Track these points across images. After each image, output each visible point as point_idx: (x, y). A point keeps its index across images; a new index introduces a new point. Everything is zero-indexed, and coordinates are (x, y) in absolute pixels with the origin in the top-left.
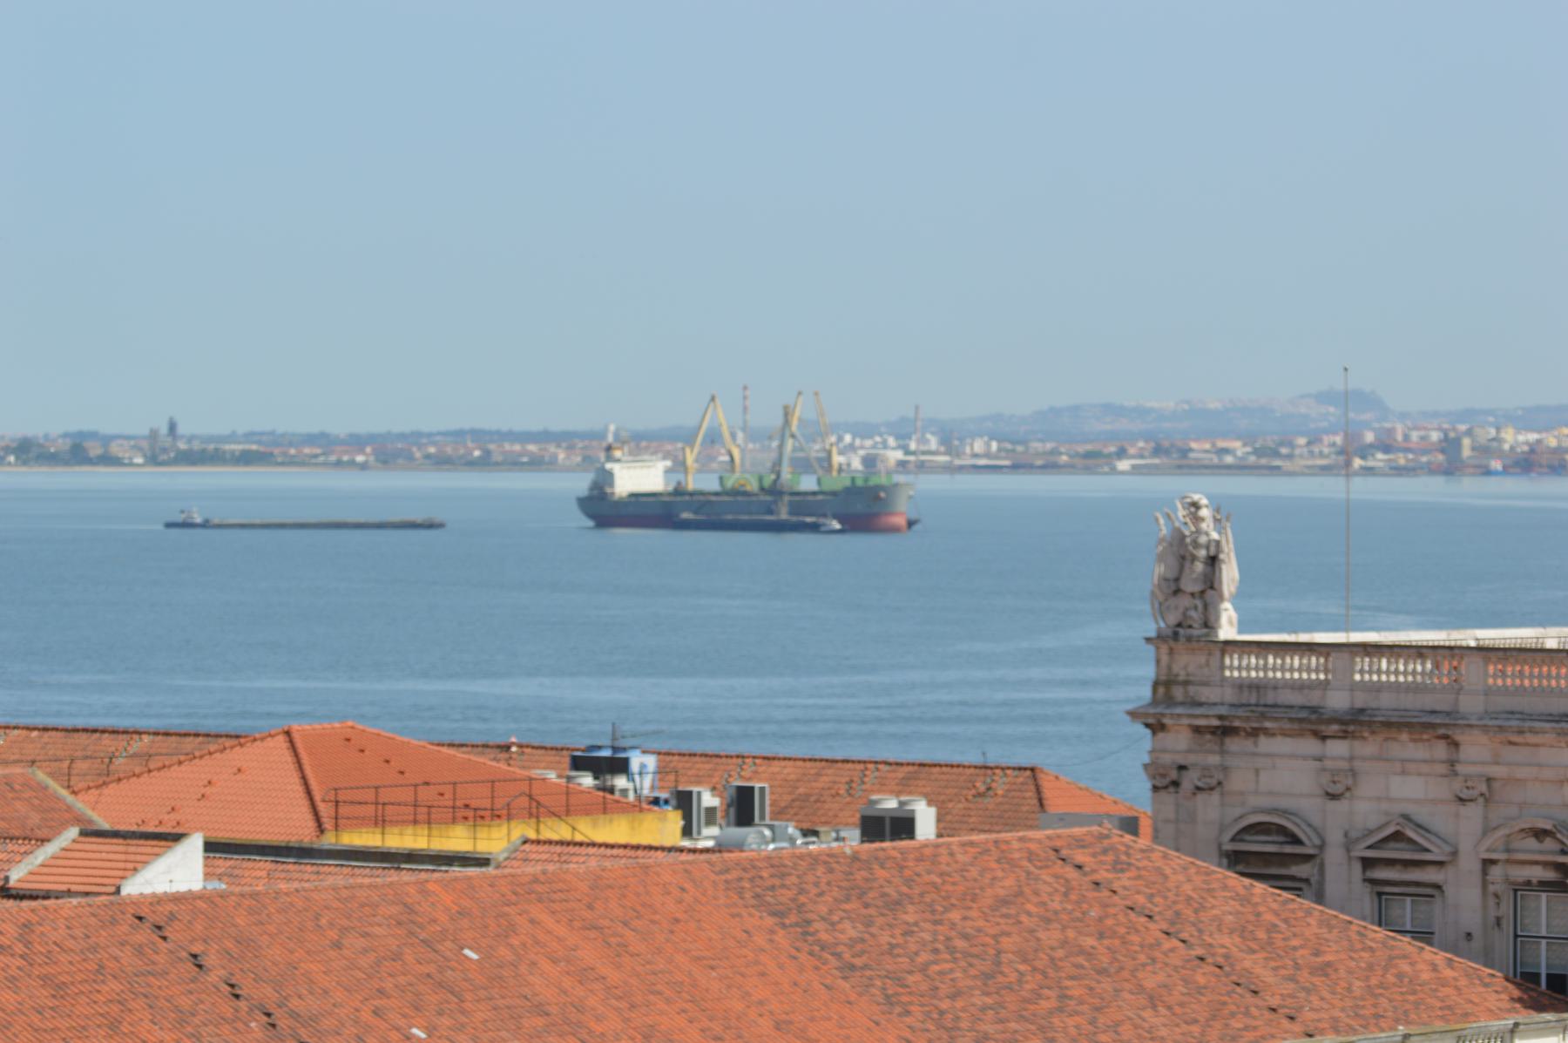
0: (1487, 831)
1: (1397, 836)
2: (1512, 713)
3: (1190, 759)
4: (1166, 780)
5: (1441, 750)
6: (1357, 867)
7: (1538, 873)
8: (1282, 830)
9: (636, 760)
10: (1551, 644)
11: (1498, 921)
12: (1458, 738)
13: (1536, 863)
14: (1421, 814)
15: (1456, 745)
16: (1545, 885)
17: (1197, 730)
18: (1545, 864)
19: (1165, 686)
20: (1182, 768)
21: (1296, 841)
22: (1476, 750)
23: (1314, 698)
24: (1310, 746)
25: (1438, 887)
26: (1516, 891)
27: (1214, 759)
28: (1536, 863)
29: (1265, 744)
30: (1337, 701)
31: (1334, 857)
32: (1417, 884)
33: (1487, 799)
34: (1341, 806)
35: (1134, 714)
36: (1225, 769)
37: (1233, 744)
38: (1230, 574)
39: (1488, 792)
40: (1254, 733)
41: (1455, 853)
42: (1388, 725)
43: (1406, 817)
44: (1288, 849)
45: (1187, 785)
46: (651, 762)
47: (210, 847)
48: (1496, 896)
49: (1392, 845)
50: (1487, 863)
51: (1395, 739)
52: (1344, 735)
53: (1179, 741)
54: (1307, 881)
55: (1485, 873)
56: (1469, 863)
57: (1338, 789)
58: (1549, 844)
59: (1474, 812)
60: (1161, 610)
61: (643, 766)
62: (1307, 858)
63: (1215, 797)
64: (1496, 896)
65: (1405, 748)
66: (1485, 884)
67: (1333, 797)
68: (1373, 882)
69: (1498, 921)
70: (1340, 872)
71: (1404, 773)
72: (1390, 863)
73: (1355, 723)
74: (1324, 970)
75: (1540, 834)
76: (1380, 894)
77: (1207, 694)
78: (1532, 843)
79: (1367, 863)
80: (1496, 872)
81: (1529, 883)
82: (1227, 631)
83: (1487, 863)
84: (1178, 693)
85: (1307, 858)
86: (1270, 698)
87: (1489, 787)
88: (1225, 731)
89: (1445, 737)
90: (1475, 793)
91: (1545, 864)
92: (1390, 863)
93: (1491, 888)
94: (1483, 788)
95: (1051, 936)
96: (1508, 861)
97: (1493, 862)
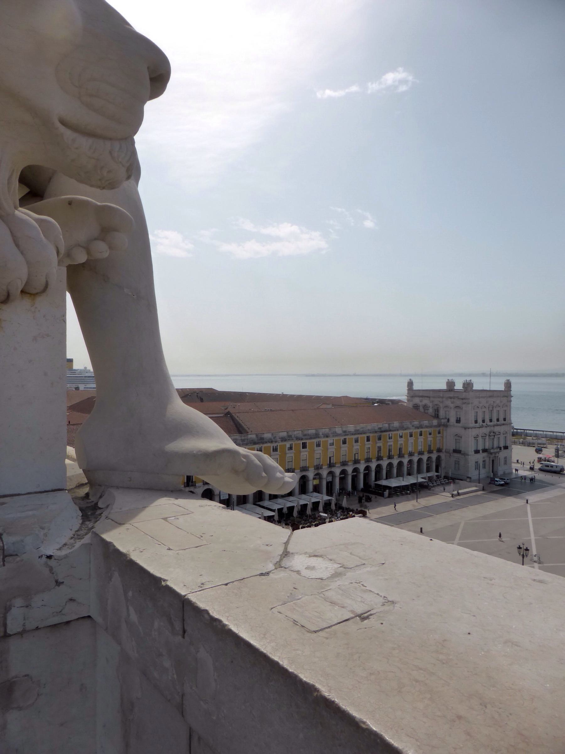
1: (425, 405)
4: (408, 400)
5: (428, 398)
7: (436, 408)
22: (432, 399)
39: (433, 402)
43: (426, 404)
47: (332, 405)
56: (431, 407)
65: (426, 398)
67: (421, 402)
73: (422, 397)
76: (424, 409)
78: (436, 406)
80: (433, 408)
85: (419, 407)
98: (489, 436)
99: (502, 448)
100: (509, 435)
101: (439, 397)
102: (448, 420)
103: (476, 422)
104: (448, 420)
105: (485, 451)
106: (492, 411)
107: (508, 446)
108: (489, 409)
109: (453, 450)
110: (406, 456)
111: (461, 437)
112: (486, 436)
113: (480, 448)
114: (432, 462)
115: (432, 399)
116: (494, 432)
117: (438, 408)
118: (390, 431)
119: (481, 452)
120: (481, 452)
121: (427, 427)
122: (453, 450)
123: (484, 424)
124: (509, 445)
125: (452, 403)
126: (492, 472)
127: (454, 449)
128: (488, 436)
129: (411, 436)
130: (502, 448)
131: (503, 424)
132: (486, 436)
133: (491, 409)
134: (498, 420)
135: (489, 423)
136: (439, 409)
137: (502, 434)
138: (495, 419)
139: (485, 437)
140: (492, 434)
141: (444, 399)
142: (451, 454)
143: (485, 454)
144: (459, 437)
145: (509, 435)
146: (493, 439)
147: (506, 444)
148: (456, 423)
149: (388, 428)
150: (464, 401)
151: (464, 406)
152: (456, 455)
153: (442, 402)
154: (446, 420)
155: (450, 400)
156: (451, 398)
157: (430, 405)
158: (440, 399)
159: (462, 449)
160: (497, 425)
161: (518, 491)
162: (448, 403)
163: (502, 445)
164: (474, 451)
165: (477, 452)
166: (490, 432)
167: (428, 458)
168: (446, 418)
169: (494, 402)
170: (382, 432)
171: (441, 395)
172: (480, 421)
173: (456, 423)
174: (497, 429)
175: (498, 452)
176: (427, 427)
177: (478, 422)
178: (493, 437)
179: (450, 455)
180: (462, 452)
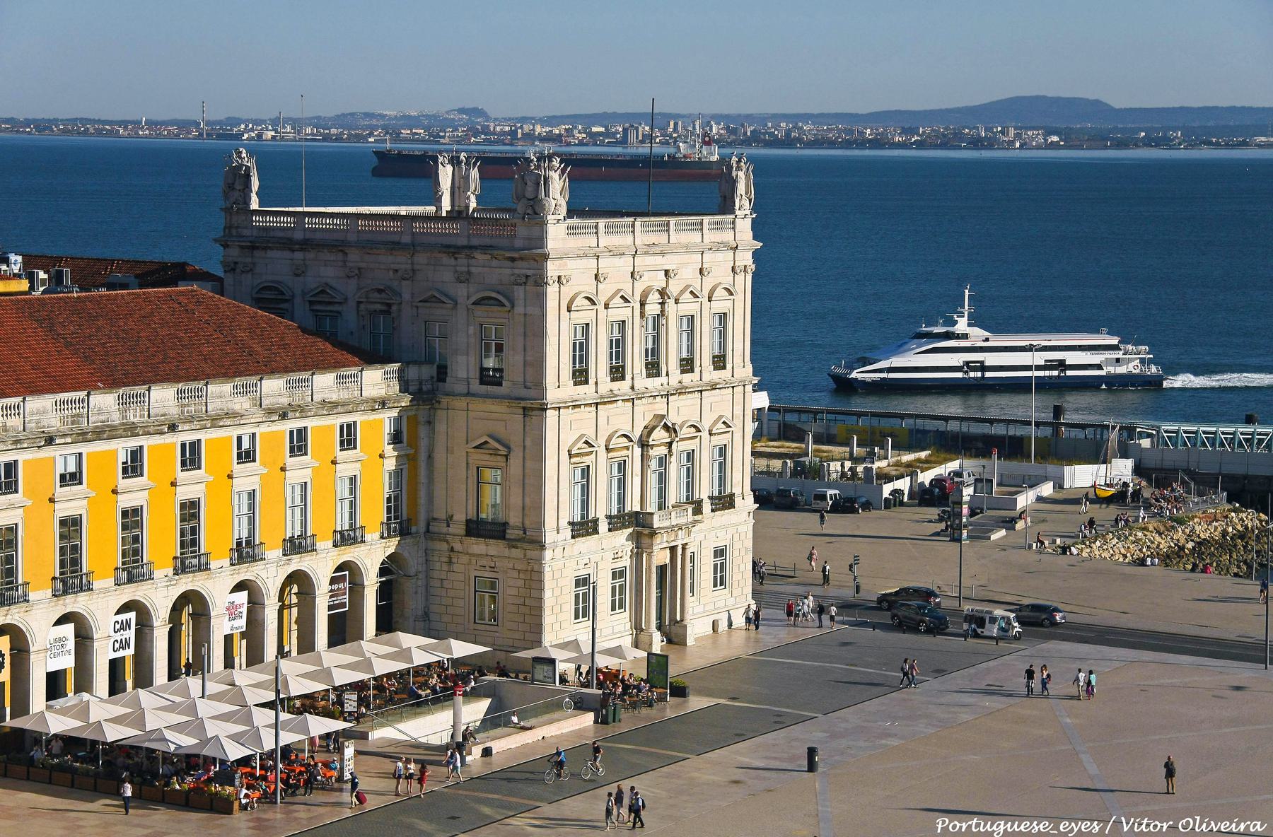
0: (359, 289)
1: (323, 292)
2: (368, 241)
3: (239, 260)
4: (231, 268)
5: (340, 256)
6: (307, 304)
7: (378, 307)
8: (277, 289)
9: (13, 257)
10: (403, 213)
11: (364, 327)
12: (347, 251)
13: (379, 303)
14: (333, 283)
15: (346, 254)
16: (382, 312)
17: (242, 247)
18: (382, 303)
19: (229, 228)
20: (236, 263)
21: (282, 293)
22: (354, 256)
23: (289, 234)
24: (287, 254)
25: (338, 312)
26: (370, 314)
27: (249, 260)
28: (379, 303)
29: (270, 254)
30: (298, 236)
31: (298, 300)
32: (331, 311)
33: (359, 276)
34: (301, 279)
35: (216, 240)
36: (254, 264)
37: (257, 253)
38: (255, 184)
39: (360, 272)
40: (265, 249)
41: (346, 299)
42: (318, 245)
43: (327, 284)
44: (280, 297)
45: (238, 270)
46: (19, 259)
48: (363, 316)
49: (321, 295)
50: (359, 303)
51: (322, 252)
52: (302, 250)
53: (234, 252)
54: (287, 310)
55: (358, 307)
56: (352, 303)
57: (300, 272)
58: (383, 295)
59: (353, 282)
60: (226, 196)
61: (16, 261)
62: (286, 301)
63: (249, 275)
64: (363, 316)
66: (358, 311)
67: (297, 275)
68: (313, 310)
69: (364, 327)
70: (300, 307)
71: (325, 265)
72: (320, 303)
74: (284, 346)
75: (380, 291)
76: (317, 316)
77: (246, 232)
78: (376, 295)
79: (311, 303)
80: (362, 307)
81: (375, 311)
82: (255, 205)
83: (359, 303)
84: (234, 232)
85: (286, 301)
86: (272, 234)
87: (360, 272)
88: (253, 248)
89: (342, 251)
90: (353, 274)
91: (382, 303)
92: (320, 303)
93: (360, 313)
94: (357, 271)
95: (161, 332)
96: (367, 302)
97: (361, 302)
98: (644, 444)
99: (707, 507)
100: (737, 437)
101: (394, 246)
102: (442, 373)
103: (581, 376)
104: (439, 367)
105: (618, 521)
106: (656, 319)
107: (732, 496)
108: (642, 314)
109: (468, 522)
110: (219, 562)
111: (506, 456)
112: (627, 448)
113: (602, 507)
114: (357, 588)
115: (354, 256)
116: (666, 427)
117: (389, 305)
118: (131, 430)
119: (603, 526)
120: (603, 526)
121: (331, 407)
122: (468, 522)
123: (623, 387)
124: (737, 491)
125: (459, 280)
126: (659, 628)
127: (472, 515)
128: (638, 451)
129: (246, 456)
130: (707, 507)
131: (713, 387)
132: (627, 448)
133: (653, 308)
134: (687, 365)
135: (643, 383)
136: (394, 308)
137: (705, 434)
138: (671, 362)
139: (625, 452)
140: (659, 435)
141: (421, 259)
142: (458, 546)
143: (621, 540)
144: (495, 453)
145: (737, 437)
146: (662, 461)
147: (722, 481)
148: (482, 382)
149: (116, 419)
150: (522, 268)
151: (519, 292)
152: (479, 546)
153: (411, 275)
154: (428, 371)
155: (446, 260)
156: (453, 250)
157: (349, 288)
158: (401, 260)
159: (514, 519)
160: (682, 391)
161: (779, 715)
162: (443, 274)
163: (705, 489)
164: (571, 523)
165: (584, 528)
166: (649, 430)
167: (339, 569)
168: (429, 360)
169: (667, 272)
170: (83, 437)
171: (406, 239)
172: (600, 364)
173: (482, 382)
174: (682, 411)
175: (688, 527)
176: (331, 407)
177: (592, 381)
178: (663, 450)
179: (452, 550)
180: (511, 533)
